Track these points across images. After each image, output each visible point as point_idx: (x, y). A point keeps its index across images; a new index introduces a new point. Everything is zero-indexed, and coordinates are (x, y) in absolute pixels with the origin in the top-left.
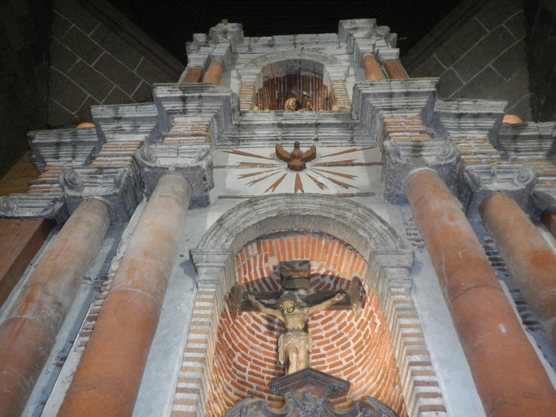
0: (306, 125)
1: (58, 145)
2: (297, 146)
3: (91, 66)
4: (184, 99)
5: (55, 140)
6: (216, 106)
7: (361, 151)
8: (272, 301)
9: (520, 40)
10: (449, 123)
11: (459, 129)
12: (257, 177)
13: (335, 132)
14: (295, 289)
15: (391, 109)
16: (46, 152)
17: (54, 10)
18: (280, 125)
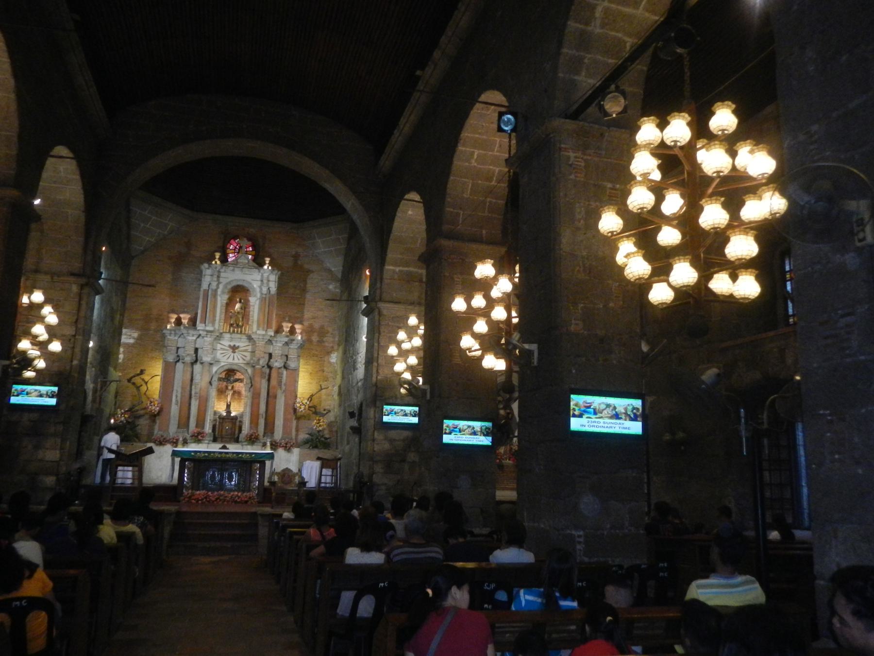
0: (238, 338)
1: (171, 334)
2: (234, 345)
3: (148, 226)
4: (207, 334)
5: (169, 332)
6: (215, 337)
7: (250, 346)
8: (226, 380)
9: (344, 247)
10: (273, 342)
11: (276, 343)
12: (225, 354)
13: (245, 340)
14: (231, 378)
15: (259, 341)
16: (167, 334)
17: (131, 208)
18: (231, 337)
